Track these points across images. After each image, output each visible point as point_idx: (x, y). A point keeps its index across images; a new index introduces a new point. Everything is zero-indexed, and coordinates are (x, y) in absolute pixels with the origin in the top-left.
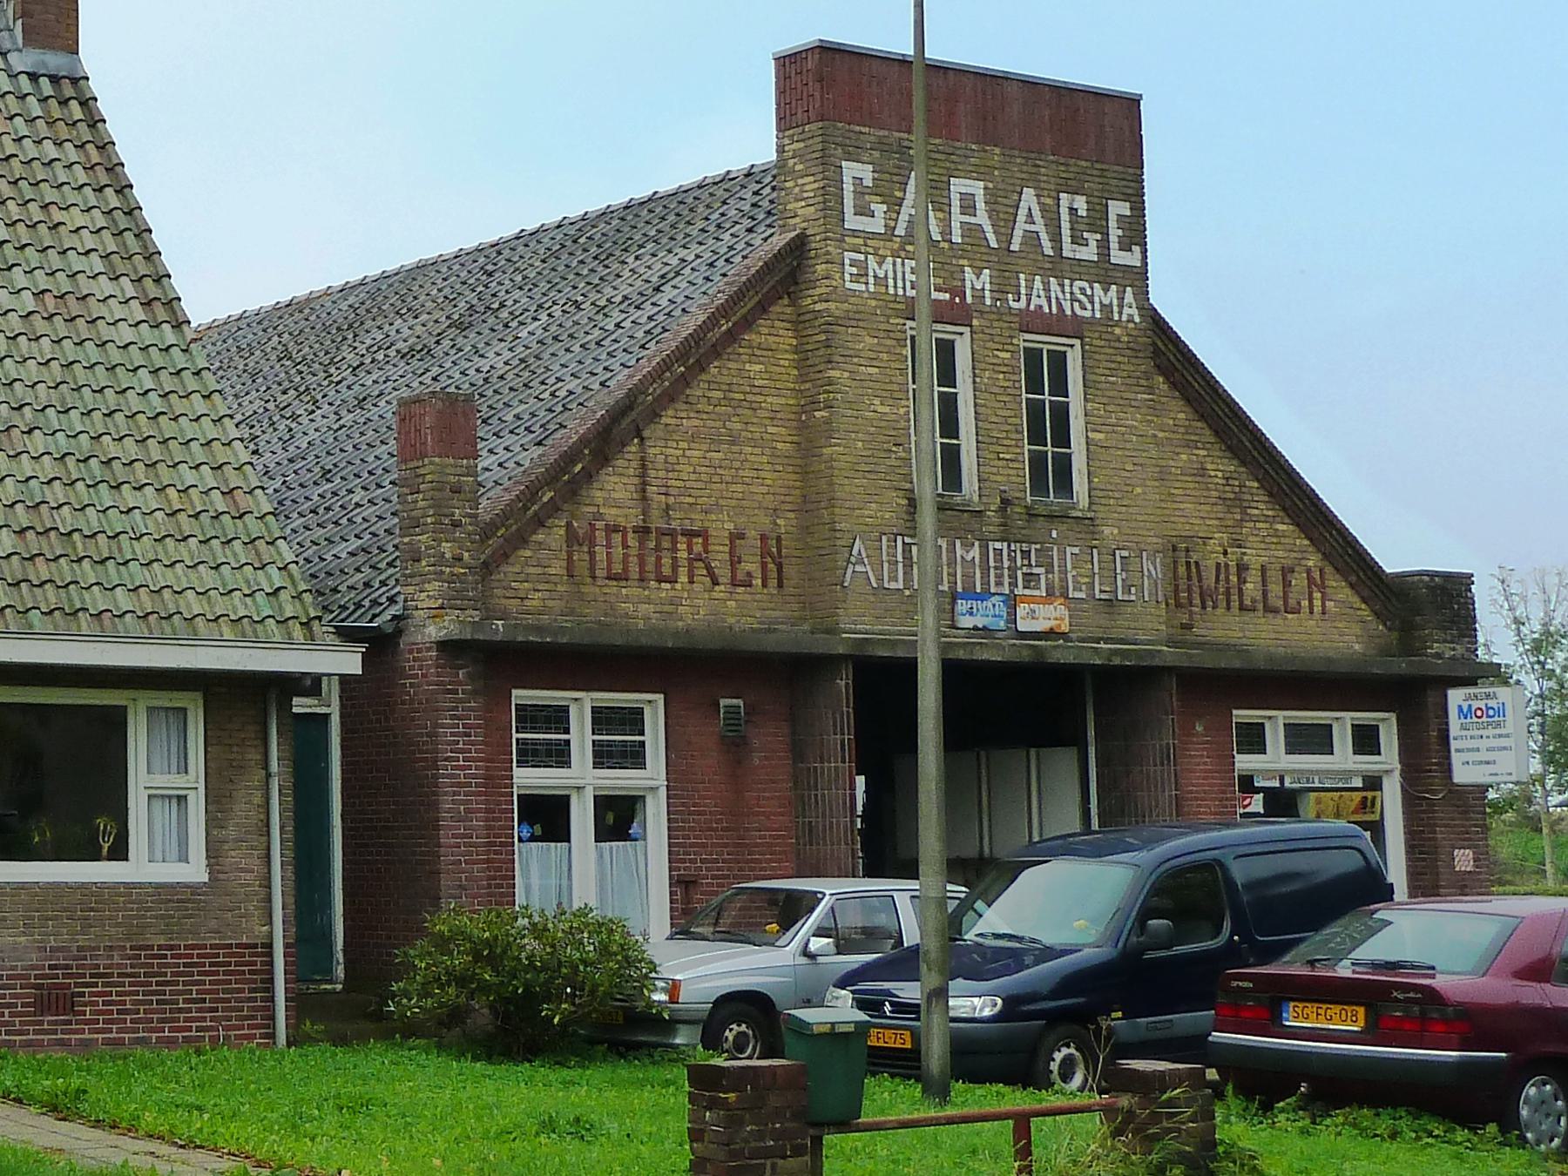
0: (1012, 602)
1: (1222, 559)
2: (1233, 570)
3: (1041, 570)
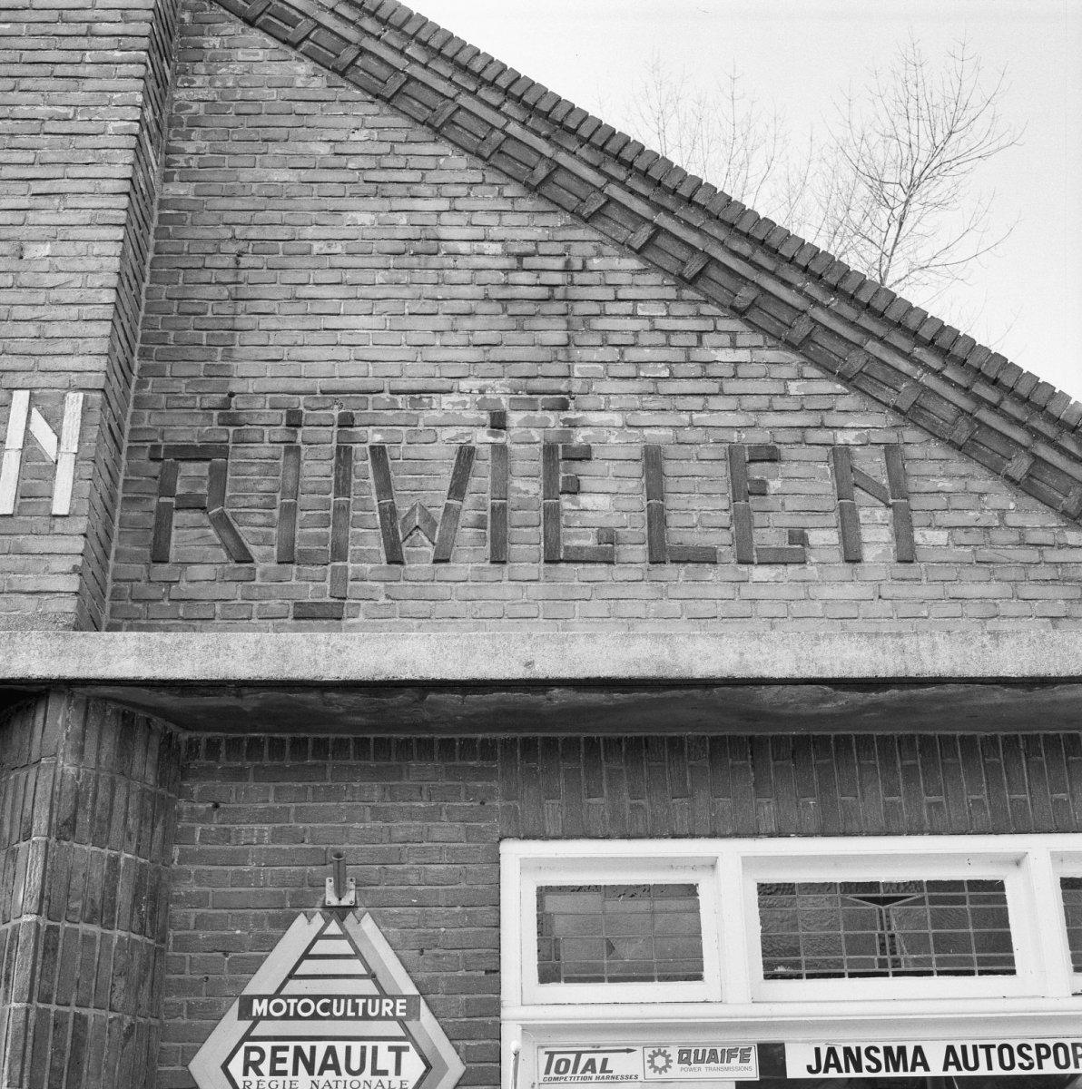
1: (482, 437)
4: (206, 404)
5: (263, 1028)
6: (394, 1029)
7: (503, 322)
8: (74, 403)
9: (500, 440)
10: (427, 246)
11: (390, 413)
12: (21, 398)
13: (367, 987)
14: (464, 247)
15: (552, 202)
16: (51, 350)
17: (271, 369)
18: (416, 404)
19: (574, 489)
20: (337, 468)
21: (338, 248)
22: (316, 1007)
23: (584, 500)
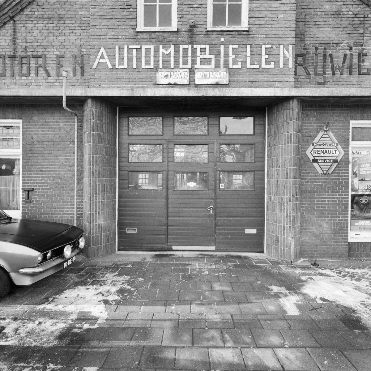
0: (192, 71)
1: (348, 52)
2: (356, 56)
3: (213, 56)
4: (301, 46)
5: (316, 147)
6: (335, 147)
7: (352, 29)
8: (291, 47)
9: (351, 52)
10: (339, 13)
11: (332, 47)
12: (282, 46)
13: (331, 142)
14: (345, 13)
15: (362, 2)
16: (285, 37)
17: (311, 39)
18: (337, 46)
19: (363, 61)
20: (324, 58)
21: (323, 13)
22: (323, 144)
23: (365, 63)
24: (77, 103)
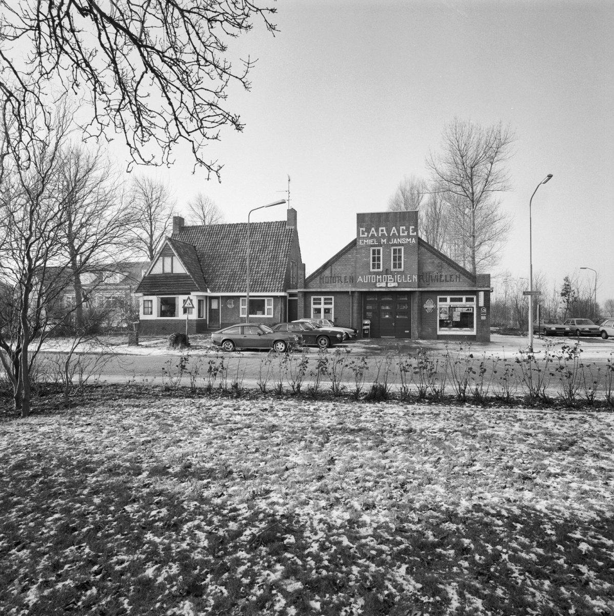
0: (387, 283)
10: (433, 263)
24: (353, 292)
